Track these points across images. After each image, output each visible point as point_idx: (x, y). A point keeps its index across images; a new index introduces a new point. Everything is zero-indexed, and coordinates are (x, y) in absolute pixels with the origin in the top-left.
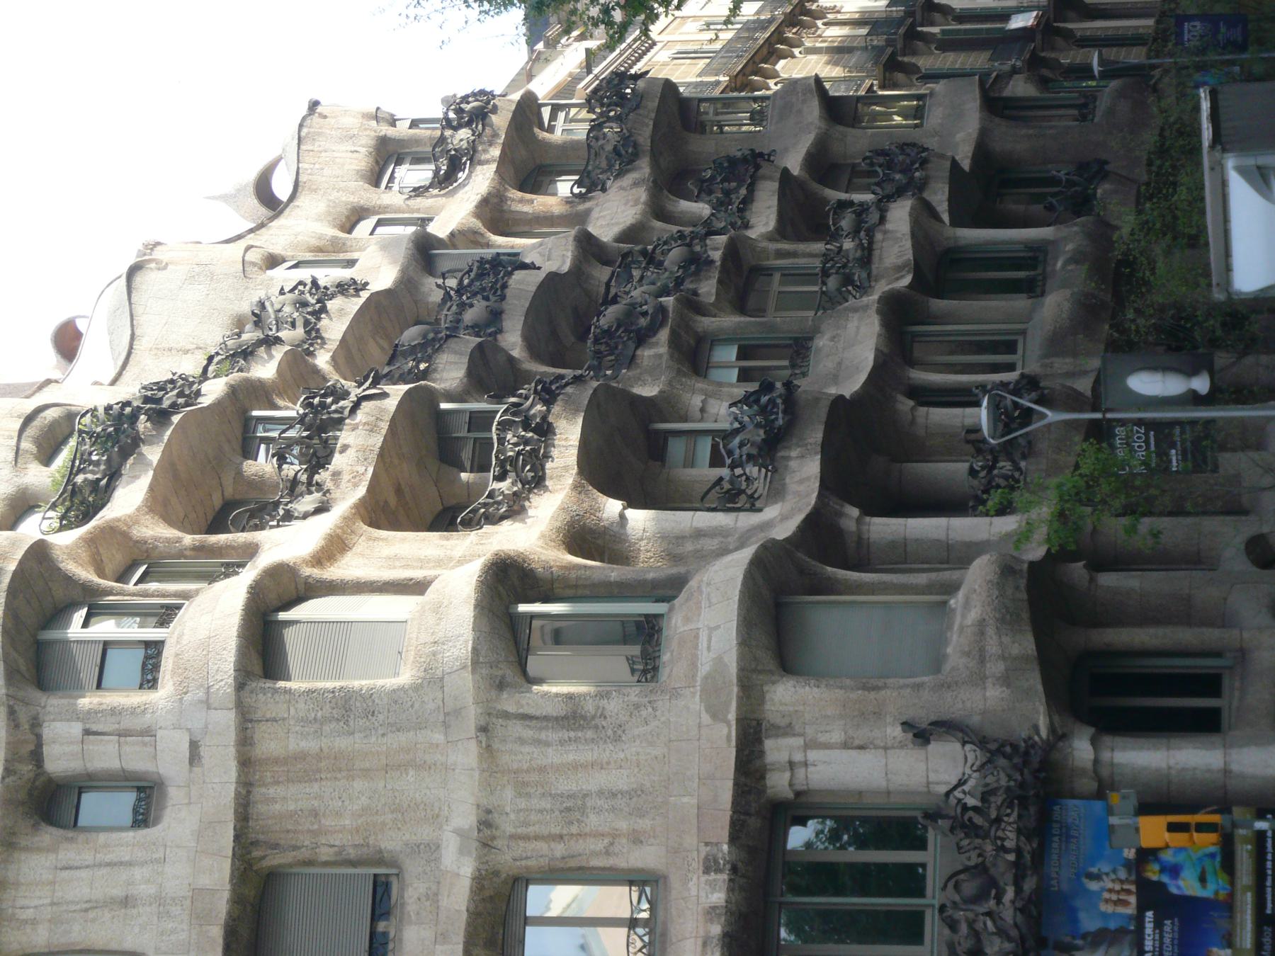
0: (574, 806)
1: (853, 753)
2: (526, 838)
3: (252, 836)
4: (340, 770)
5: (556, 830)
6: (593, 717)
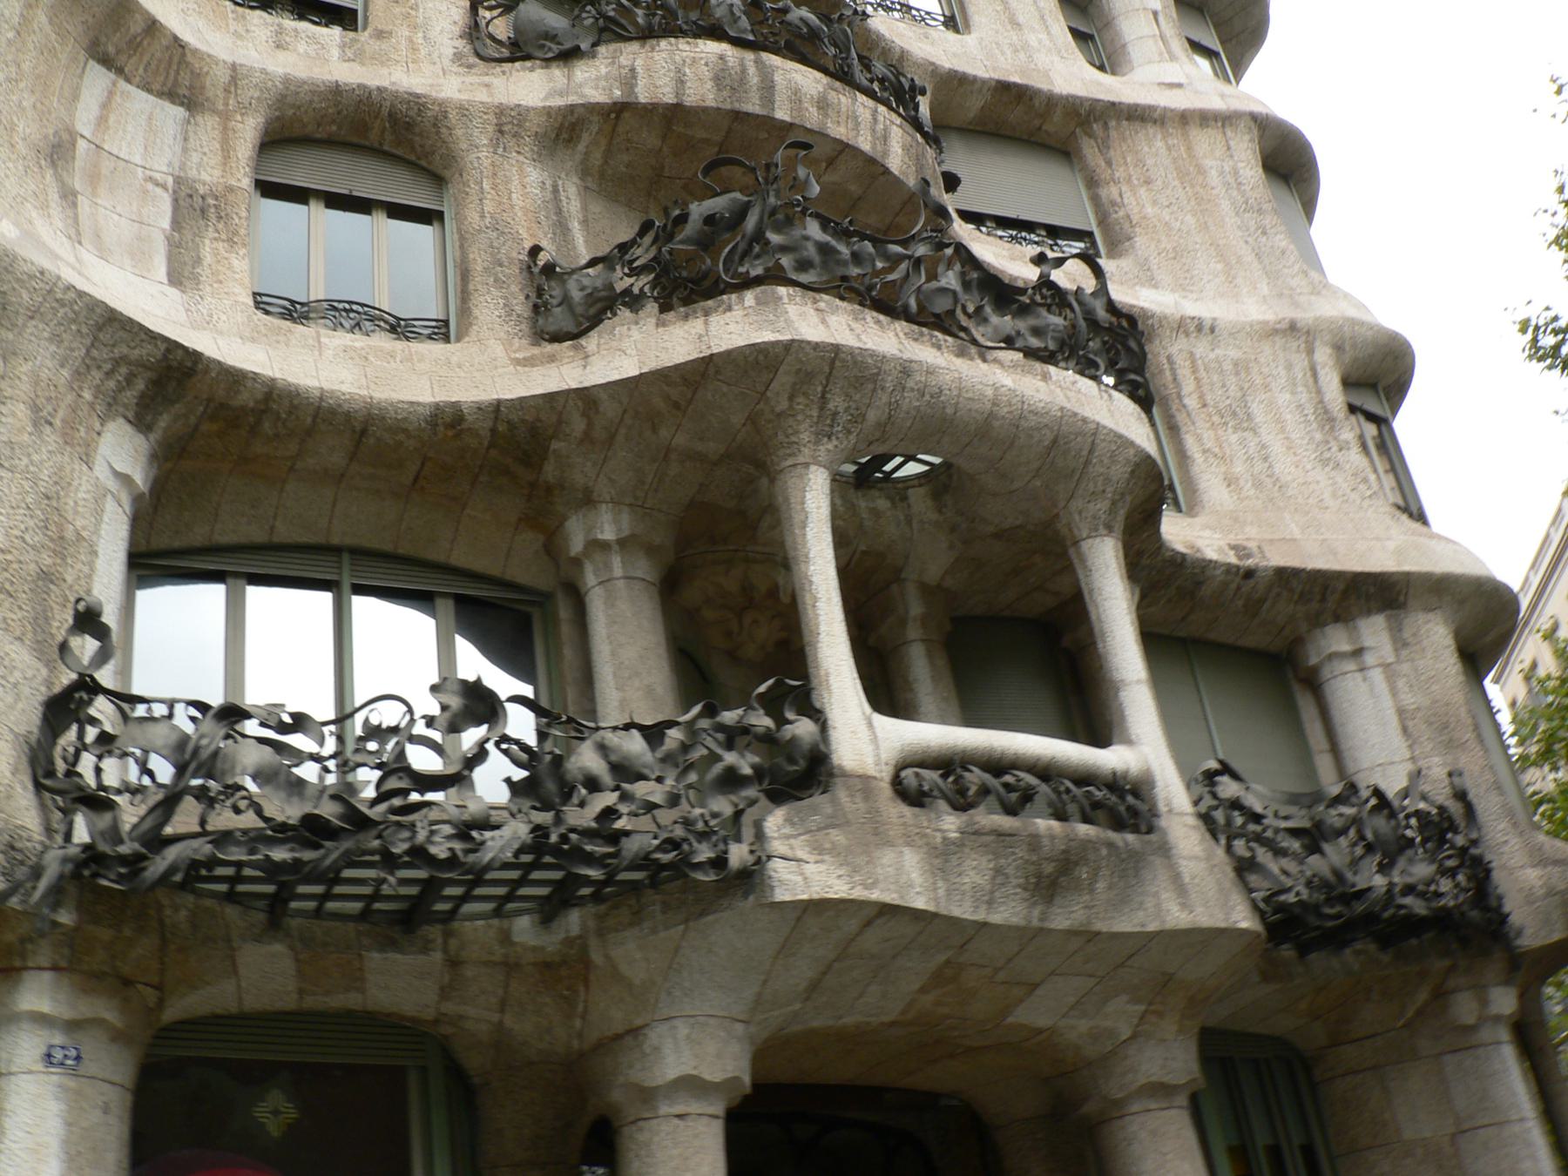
0: (1239, 417)
1: (1394, 722)
2: (1195, 370)
3: (1113, 123)
4: (1199, 204)
5: (1209, 398)
6: (1335, 438)
